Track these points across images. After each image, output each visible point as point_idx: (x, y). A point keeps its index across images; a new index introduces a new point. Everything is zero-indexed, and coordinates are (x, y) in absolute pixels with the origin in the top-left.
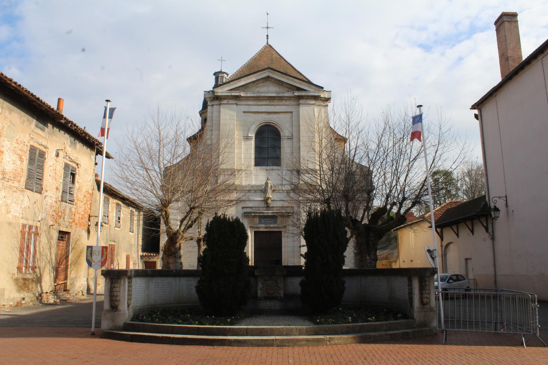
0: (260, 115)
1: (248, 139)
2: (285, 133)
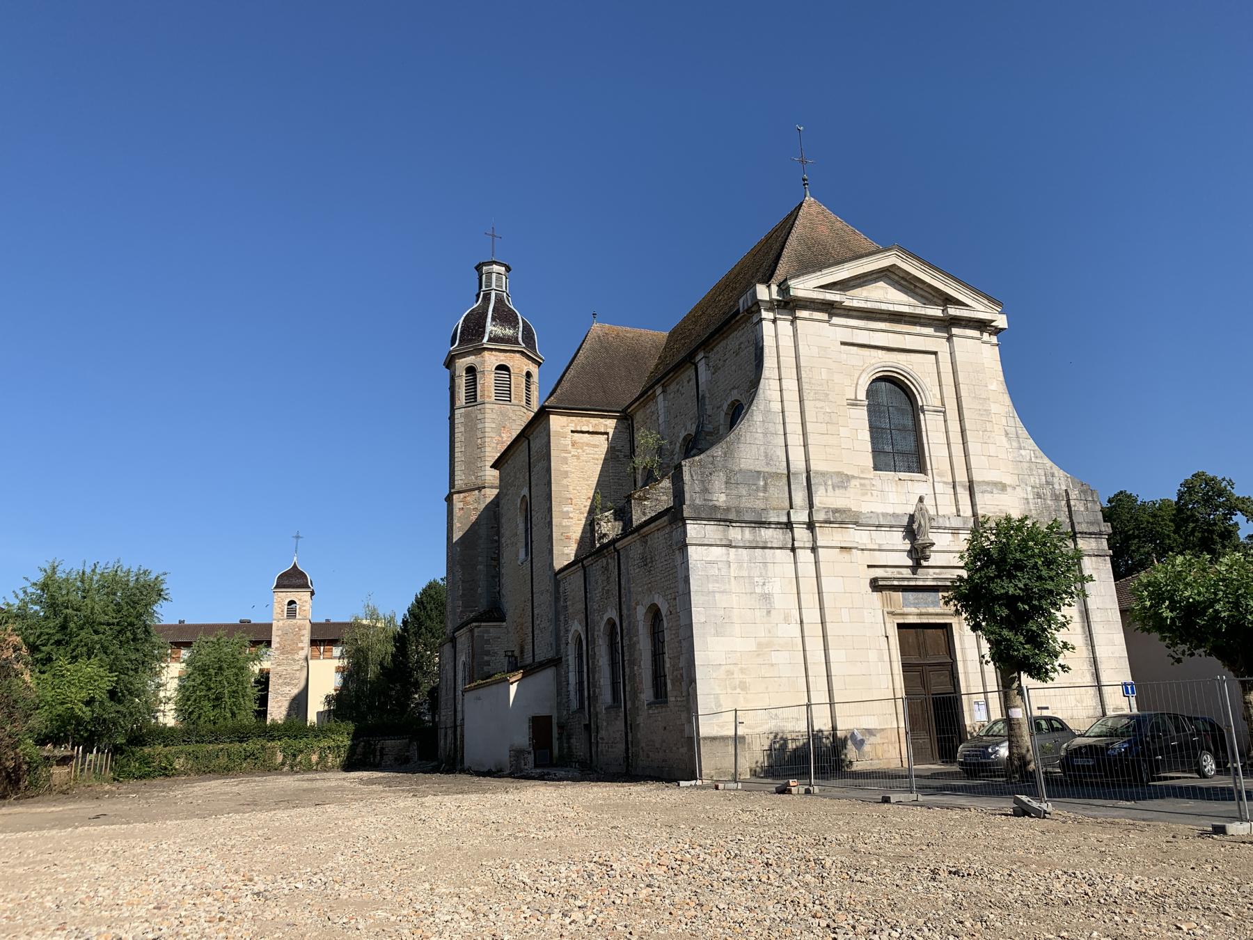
0: (874, 352)
2: (928, 395)
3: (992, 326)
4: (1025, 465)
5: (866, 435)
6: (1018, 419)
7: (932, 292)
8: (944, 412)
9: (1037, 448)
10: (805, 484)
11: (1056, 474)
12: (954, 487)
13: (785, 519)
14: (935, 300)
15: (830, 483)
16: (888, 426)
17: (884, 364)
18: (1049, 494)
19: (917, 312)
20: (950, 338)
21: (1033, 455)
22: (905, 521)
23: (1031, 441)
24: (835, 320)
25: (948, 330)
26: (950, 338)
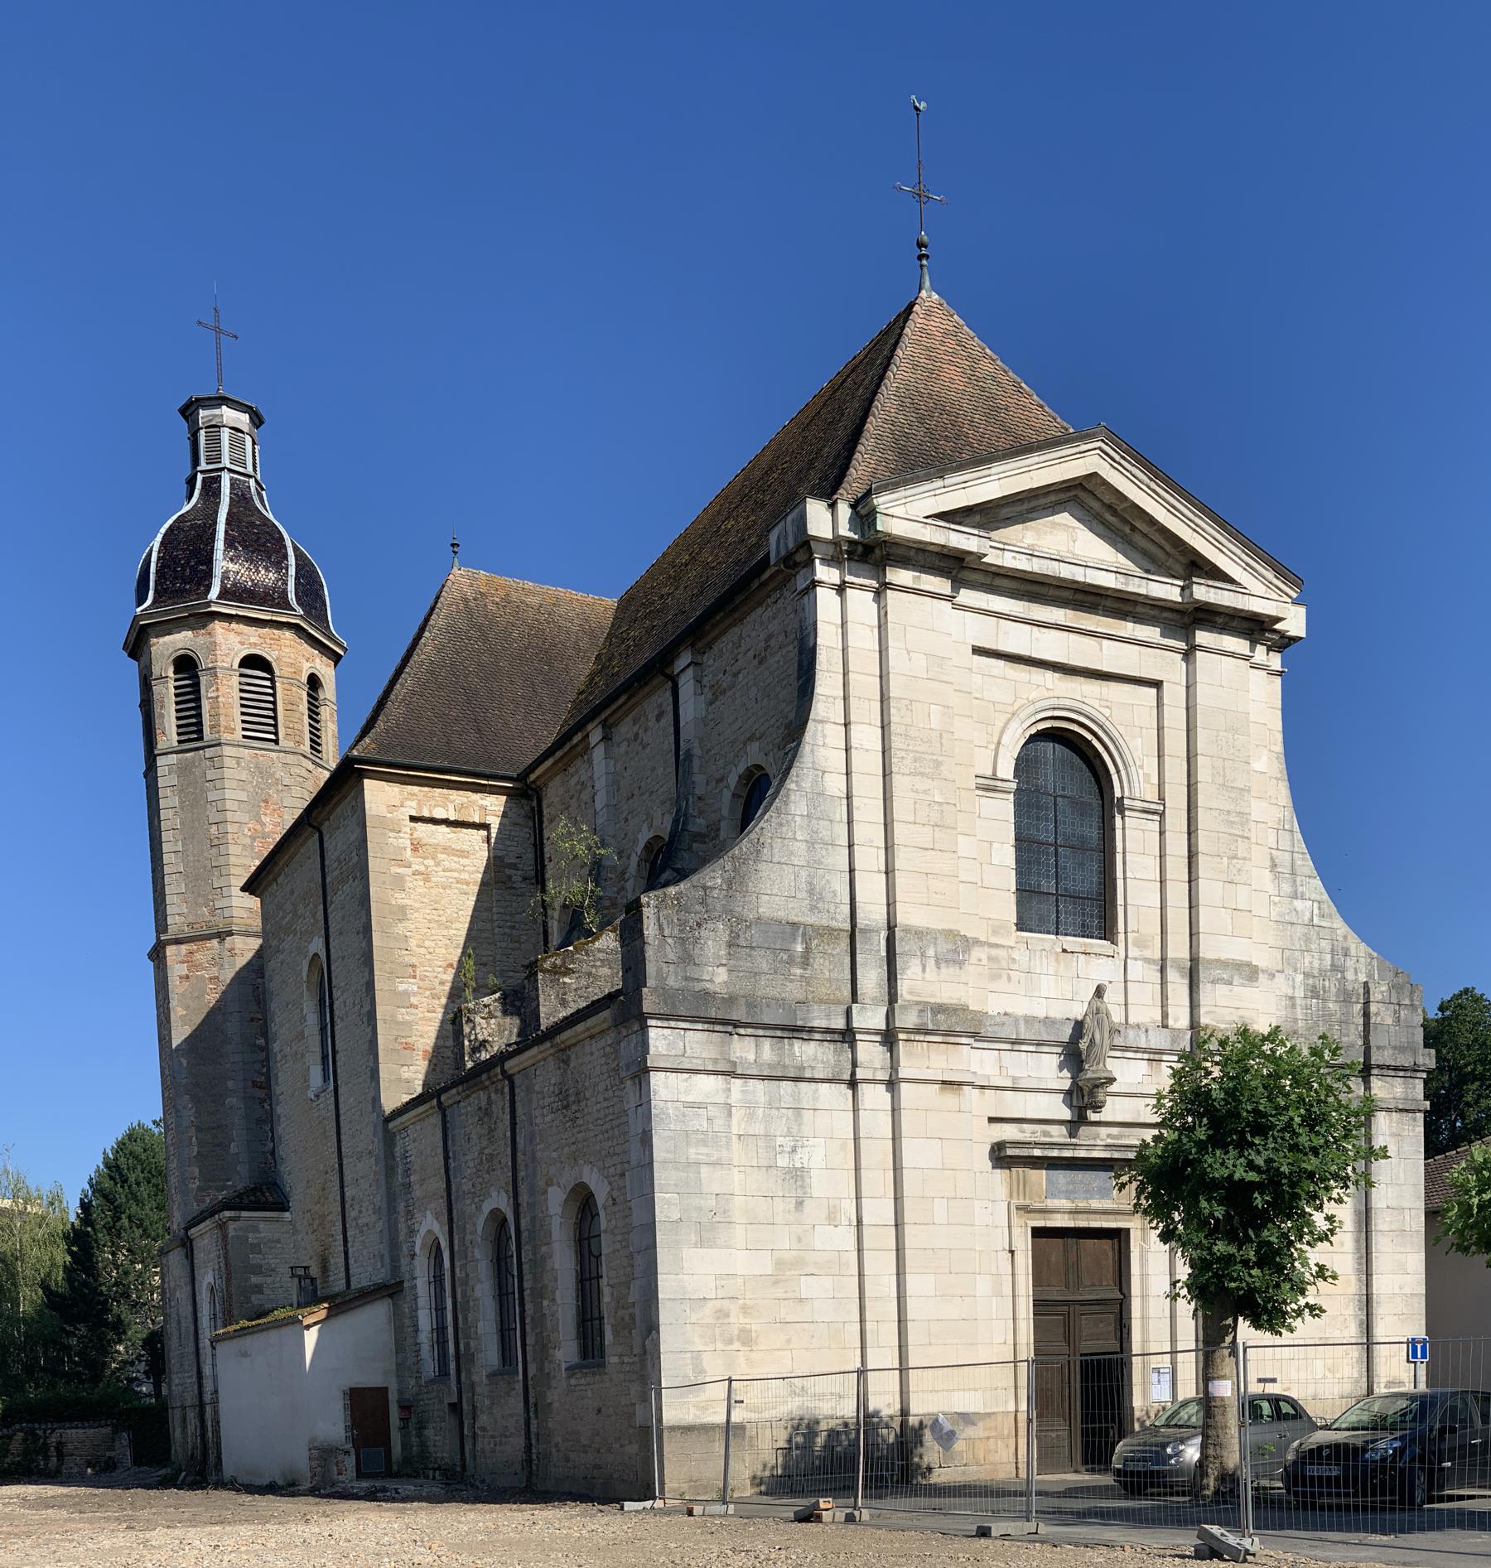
1: (994, 790)
3: (1275, 631)
4: (1300, 930)
5: (1007, 855)
7: (1168, 547)
8: (1162, 815)
9: (1326, 897)
10: (884, 954)
11: (1353, 952)
14: (1170, 562)
15: (931, 952)
17: (1055, 702)
18: (1334, 990)
19: (1130, 589)
20: (1188, 655)
21: (1316, 911)
23: (1318, 882)
25: (1189, 638)
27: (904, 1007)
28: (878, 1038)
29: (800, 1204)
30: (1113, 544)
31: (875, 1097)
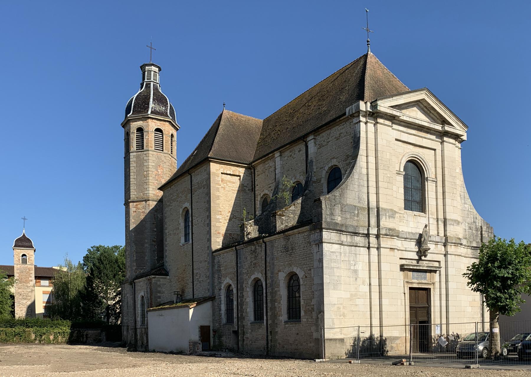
3: (460, 138)
4: (466, 212)
5: (402, 191)
6: (465, 189)
8: (436, 182)
9: (471, 204)
10: (376, 214)
12: (437, 221)
13: (366, 232)
14: (438, 121)
15: (387, 215)
16: (410, 187)
20: (442, 143)
21: (469, 208)
22: (417, 237)
23: (470, 200)
24: (395, 126)
26: (442, 143)
27: (382, 228)
28: (375, 236)
29: (356, 279)
30: (425, 115)
31: (374, 251)
